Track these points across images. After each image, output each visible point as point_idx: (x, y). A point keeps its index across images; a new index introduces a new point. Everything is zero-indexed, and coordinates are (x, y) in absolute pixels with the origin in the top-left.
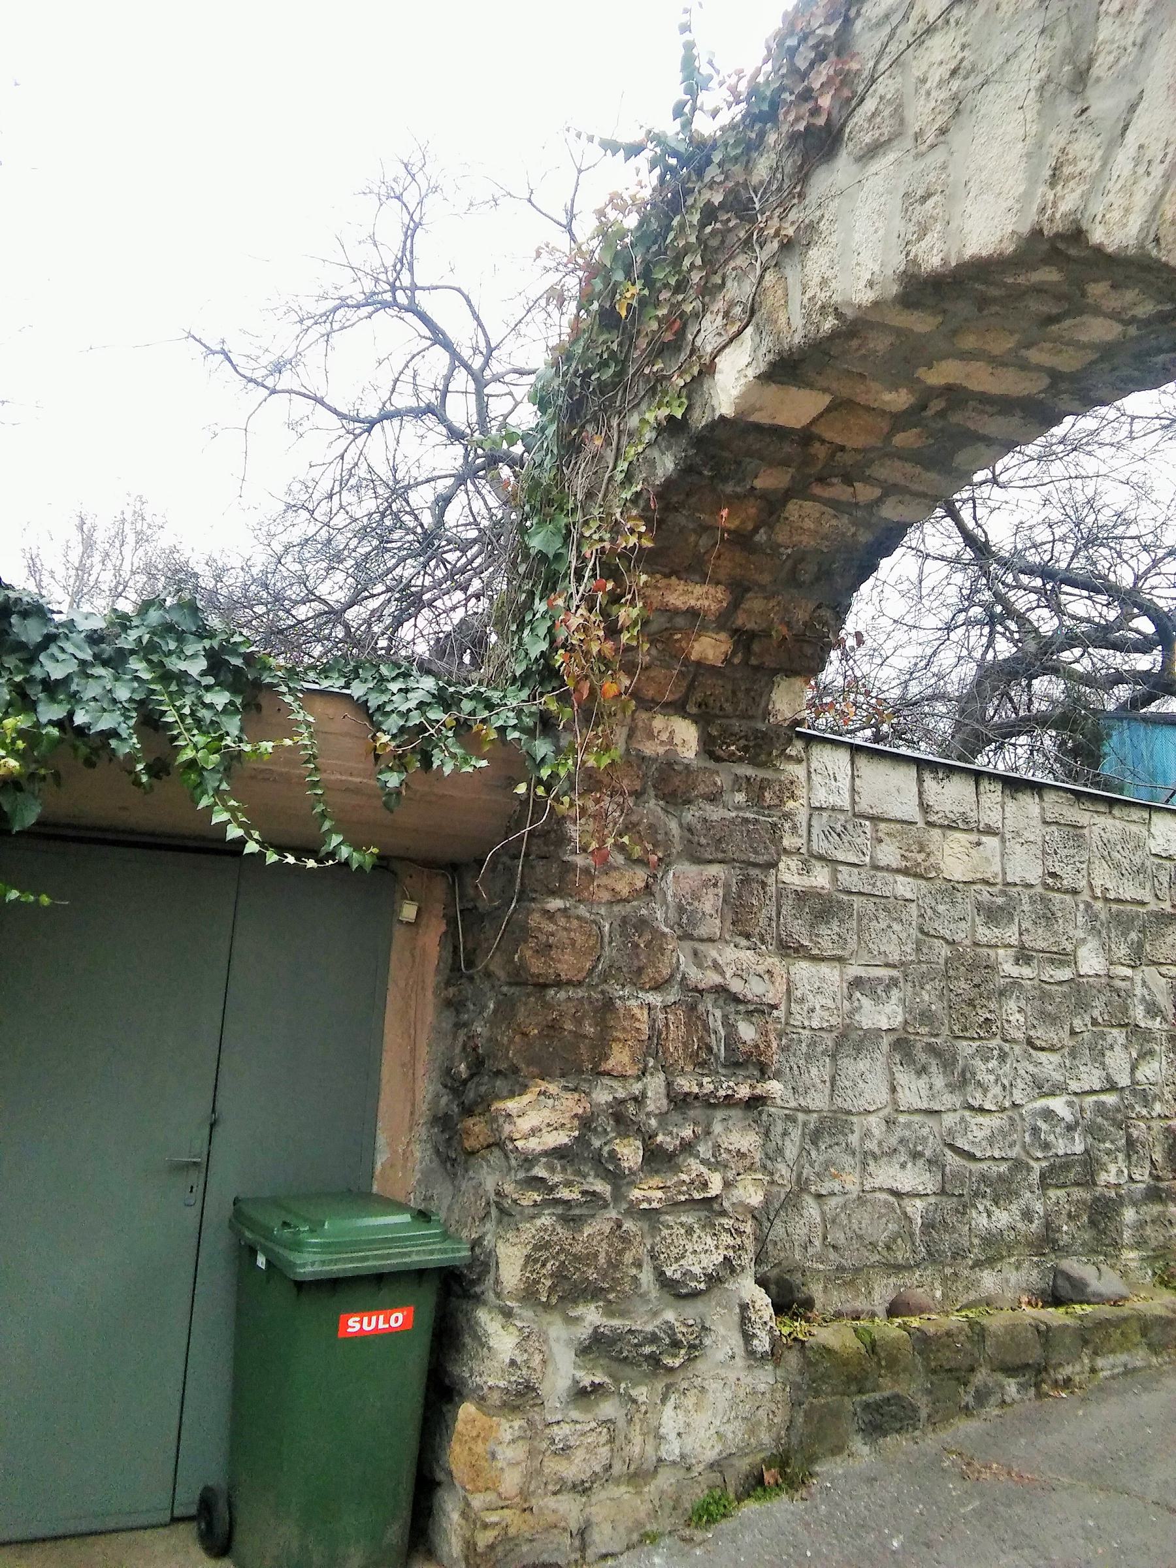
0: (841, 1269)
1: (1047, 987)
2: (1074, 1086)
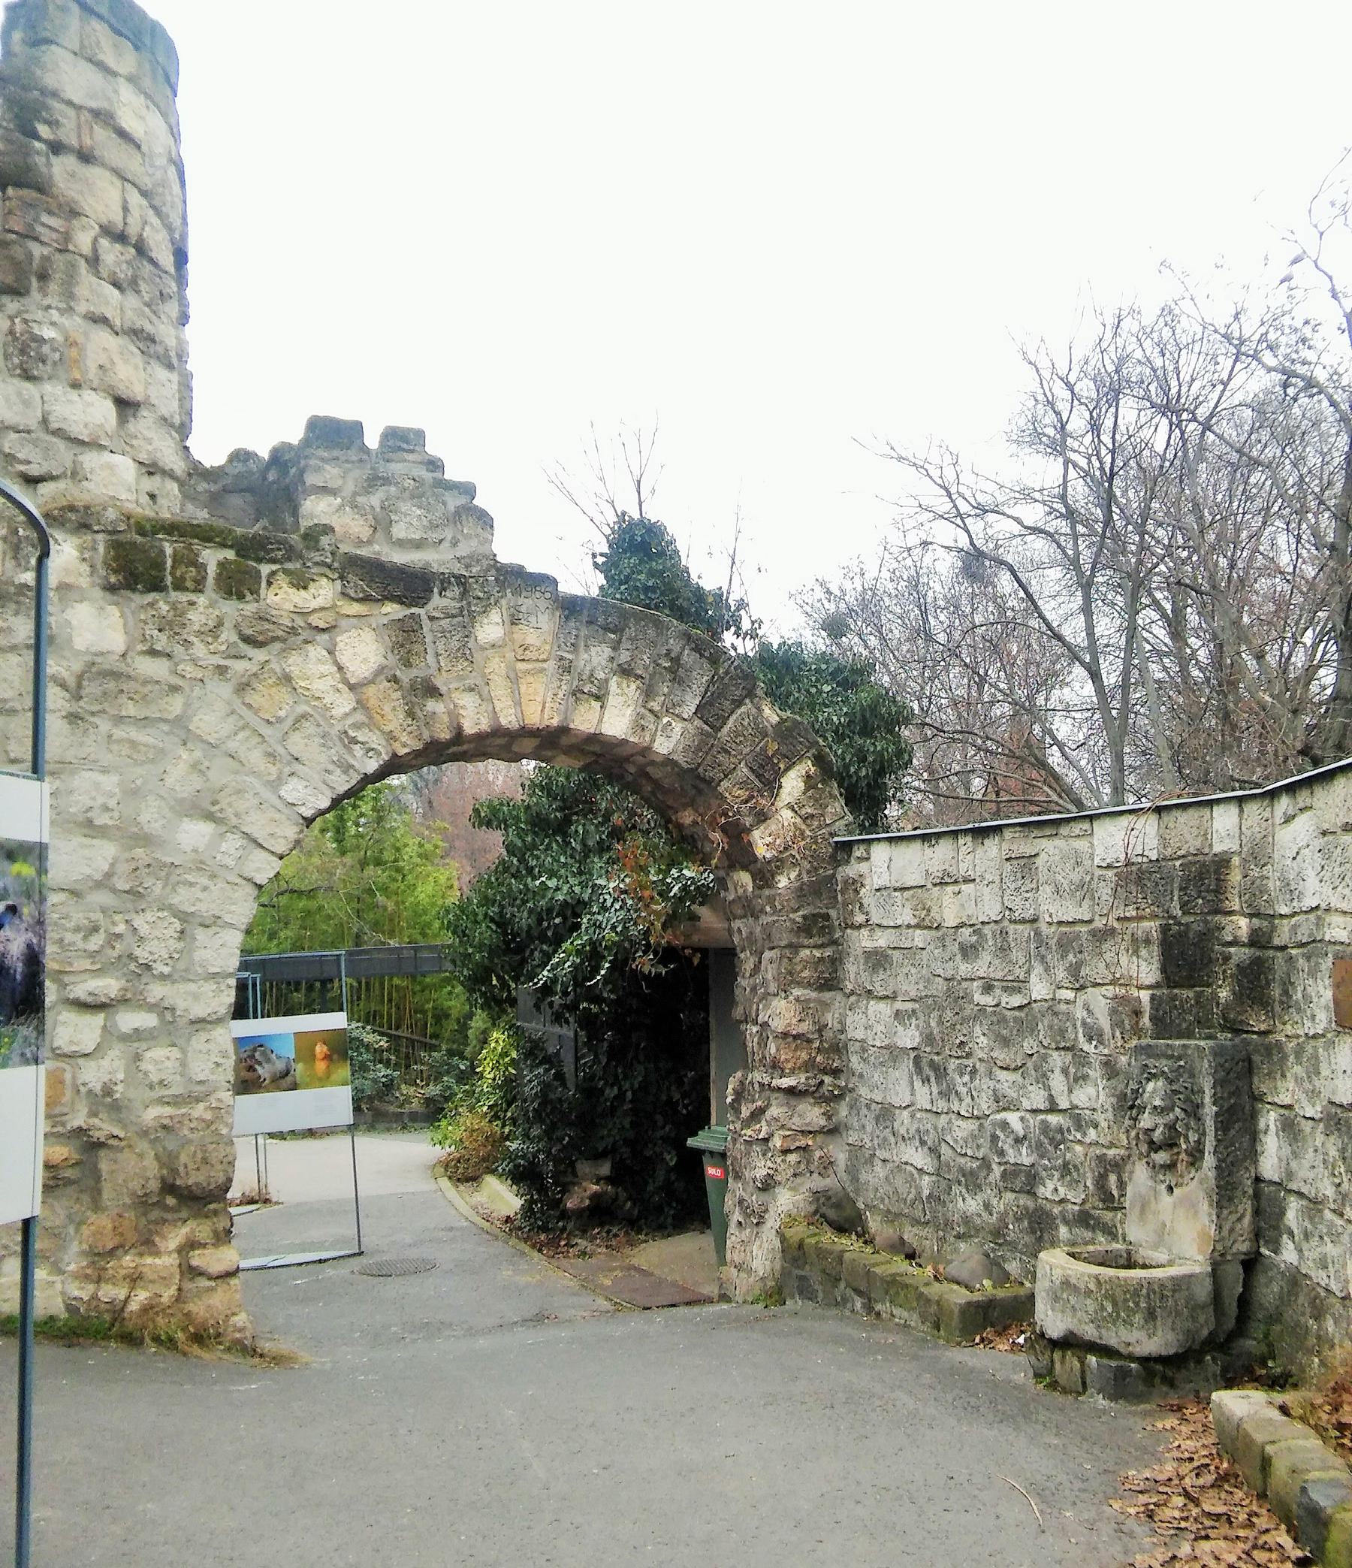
0: (889, 1211)
1: (1008, 1013)
2: (1026, 1104)
